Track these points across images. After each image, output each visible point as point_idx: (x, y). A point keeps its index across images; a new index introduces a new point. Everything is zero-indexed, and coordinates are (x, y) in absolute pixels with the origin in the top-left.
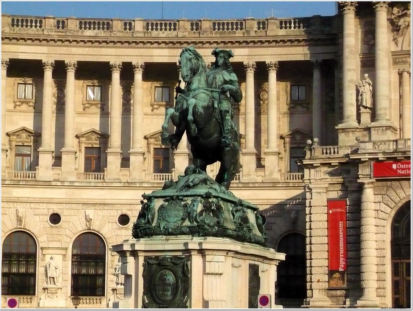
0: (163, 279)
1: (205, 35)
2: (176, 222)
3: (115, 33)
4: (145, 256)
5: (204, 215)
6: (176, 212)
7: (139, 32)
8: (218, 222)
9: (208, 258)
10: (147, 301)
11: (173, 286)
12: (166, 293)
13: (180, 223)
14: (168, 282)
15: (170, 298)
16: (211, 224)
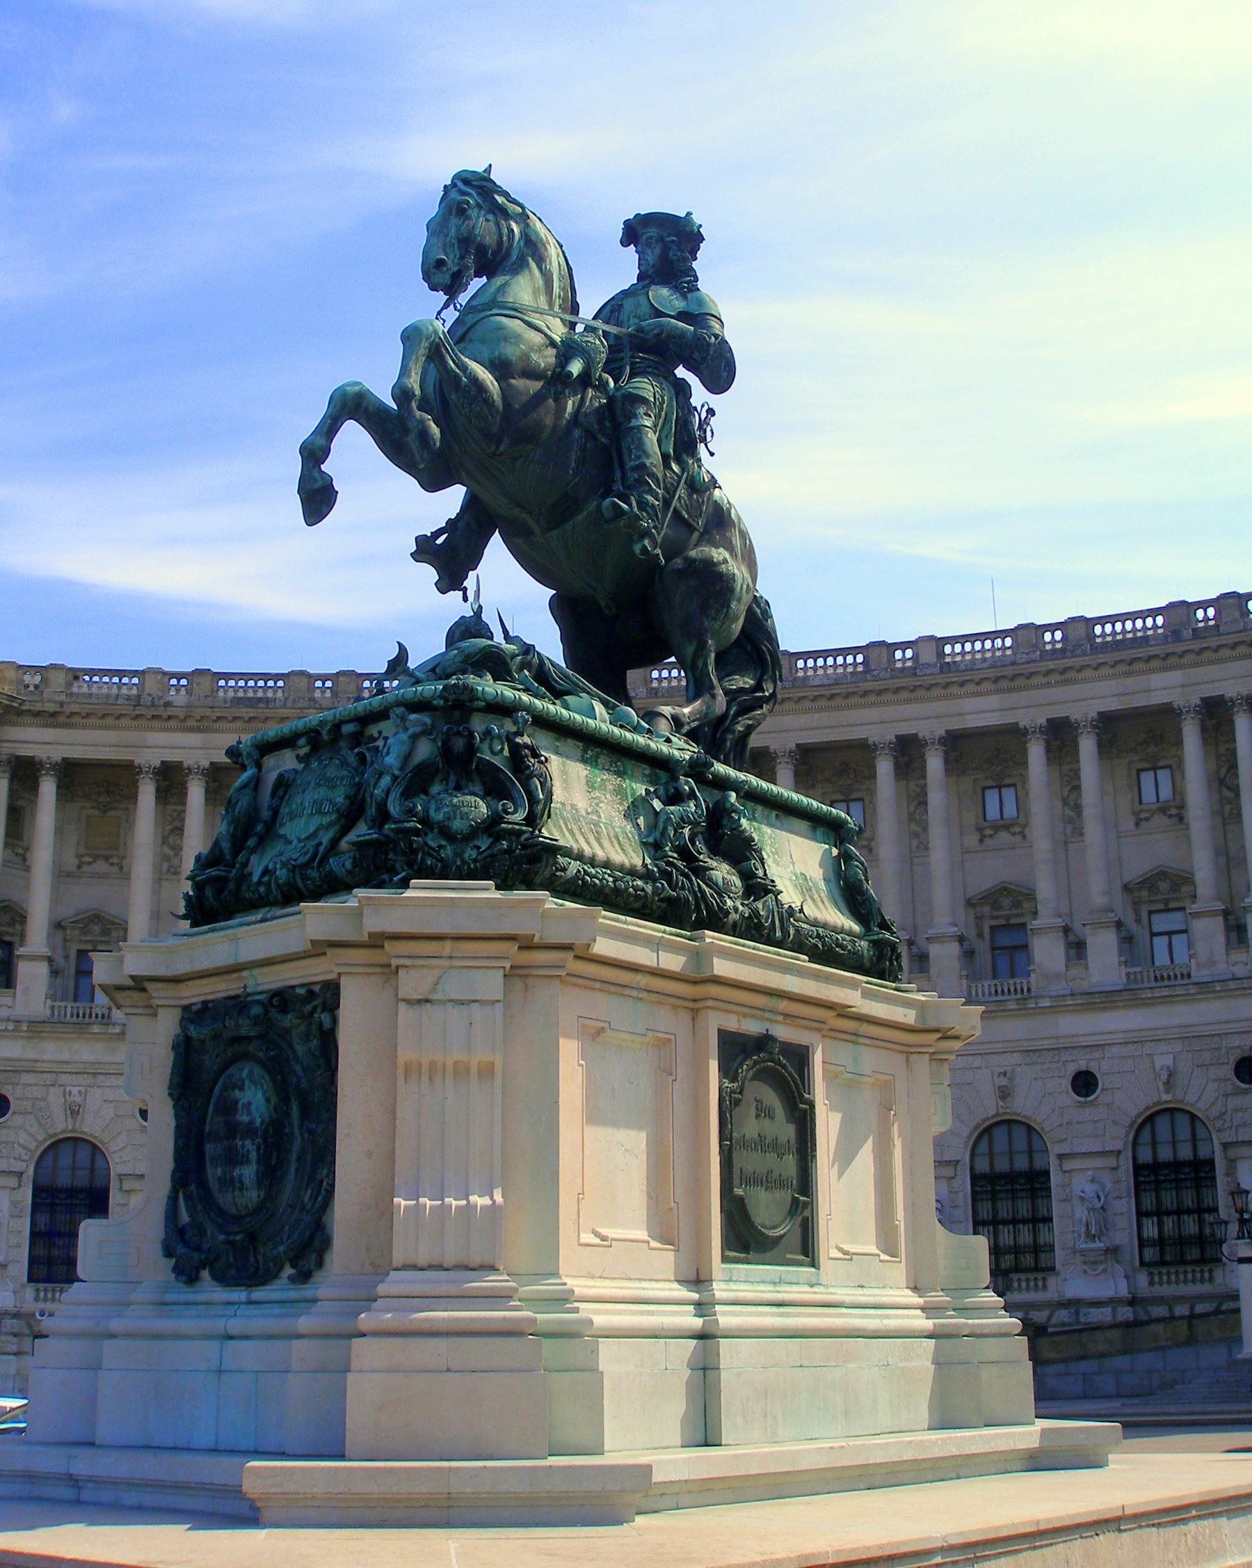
0: (228, 1108)
1: (1078, 652)
2: (315, 834)
3: (875, 673)
4: (186, 1008)
5: (436, 789)
6: (322, 792)
7: (928, 665)
8: (495, 820)
9: (411, 983)
10: (185, 1218)
11: (266, 1132)
12: (237, 1172)
13: (326, 839)
14: (244, 1118)
15: (252, 1196)
16: (457, 825)
